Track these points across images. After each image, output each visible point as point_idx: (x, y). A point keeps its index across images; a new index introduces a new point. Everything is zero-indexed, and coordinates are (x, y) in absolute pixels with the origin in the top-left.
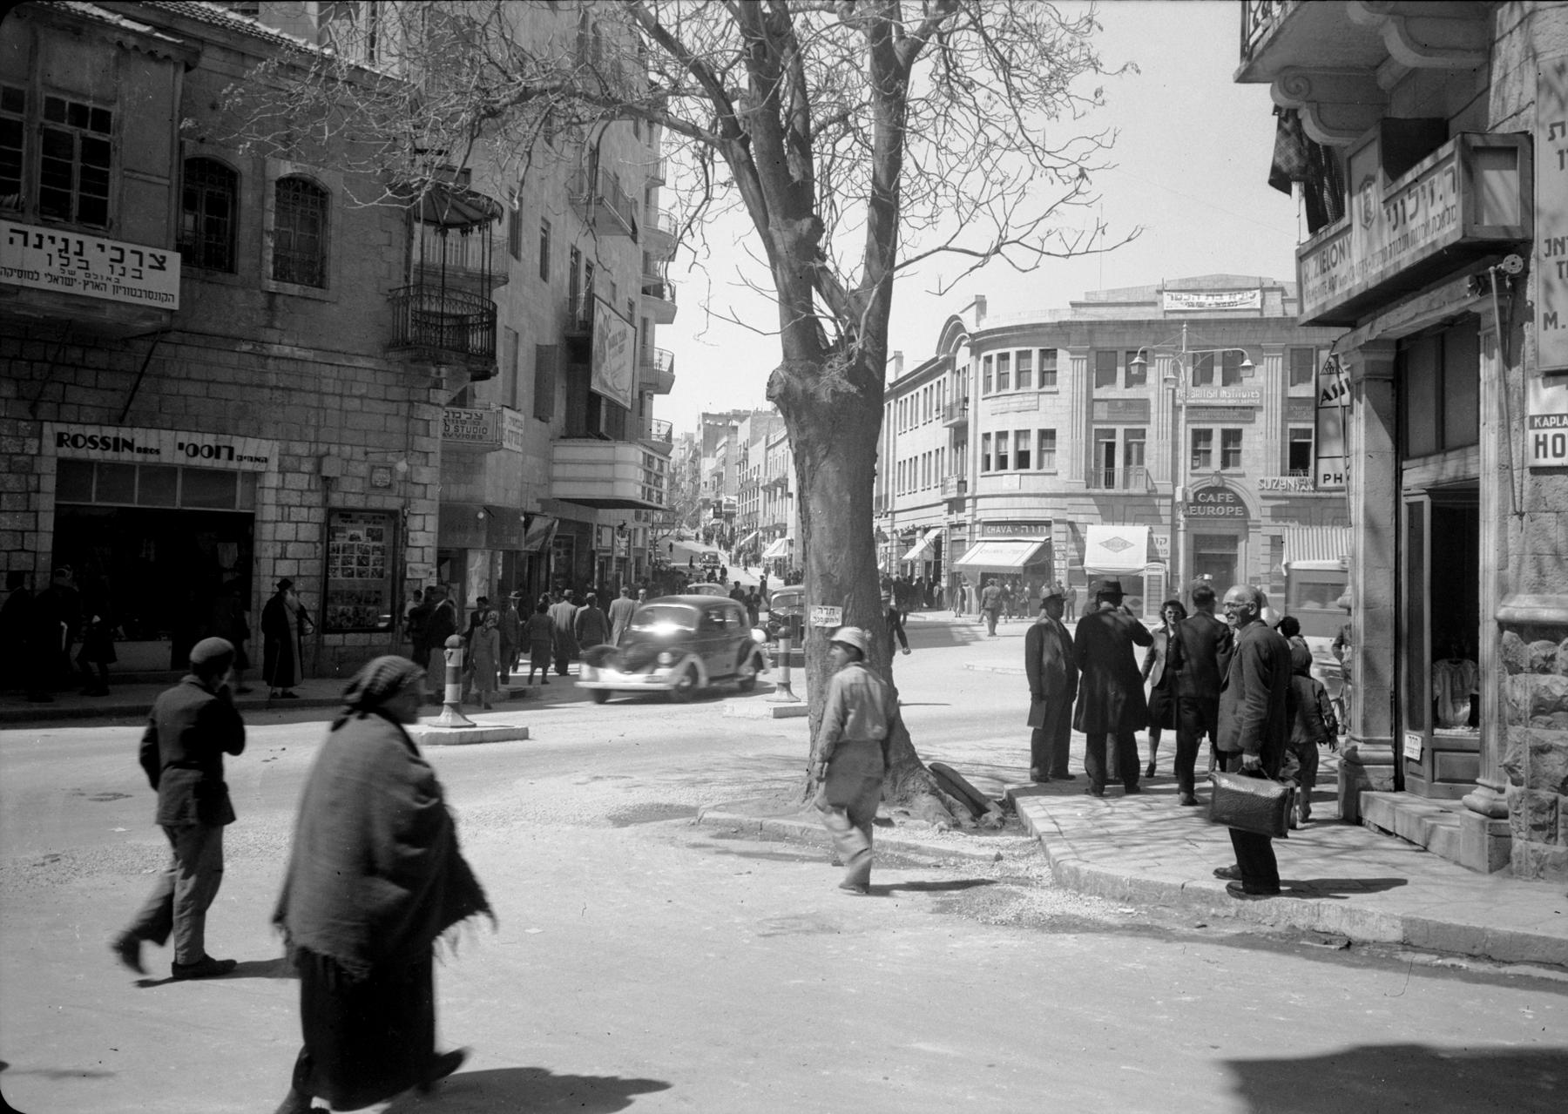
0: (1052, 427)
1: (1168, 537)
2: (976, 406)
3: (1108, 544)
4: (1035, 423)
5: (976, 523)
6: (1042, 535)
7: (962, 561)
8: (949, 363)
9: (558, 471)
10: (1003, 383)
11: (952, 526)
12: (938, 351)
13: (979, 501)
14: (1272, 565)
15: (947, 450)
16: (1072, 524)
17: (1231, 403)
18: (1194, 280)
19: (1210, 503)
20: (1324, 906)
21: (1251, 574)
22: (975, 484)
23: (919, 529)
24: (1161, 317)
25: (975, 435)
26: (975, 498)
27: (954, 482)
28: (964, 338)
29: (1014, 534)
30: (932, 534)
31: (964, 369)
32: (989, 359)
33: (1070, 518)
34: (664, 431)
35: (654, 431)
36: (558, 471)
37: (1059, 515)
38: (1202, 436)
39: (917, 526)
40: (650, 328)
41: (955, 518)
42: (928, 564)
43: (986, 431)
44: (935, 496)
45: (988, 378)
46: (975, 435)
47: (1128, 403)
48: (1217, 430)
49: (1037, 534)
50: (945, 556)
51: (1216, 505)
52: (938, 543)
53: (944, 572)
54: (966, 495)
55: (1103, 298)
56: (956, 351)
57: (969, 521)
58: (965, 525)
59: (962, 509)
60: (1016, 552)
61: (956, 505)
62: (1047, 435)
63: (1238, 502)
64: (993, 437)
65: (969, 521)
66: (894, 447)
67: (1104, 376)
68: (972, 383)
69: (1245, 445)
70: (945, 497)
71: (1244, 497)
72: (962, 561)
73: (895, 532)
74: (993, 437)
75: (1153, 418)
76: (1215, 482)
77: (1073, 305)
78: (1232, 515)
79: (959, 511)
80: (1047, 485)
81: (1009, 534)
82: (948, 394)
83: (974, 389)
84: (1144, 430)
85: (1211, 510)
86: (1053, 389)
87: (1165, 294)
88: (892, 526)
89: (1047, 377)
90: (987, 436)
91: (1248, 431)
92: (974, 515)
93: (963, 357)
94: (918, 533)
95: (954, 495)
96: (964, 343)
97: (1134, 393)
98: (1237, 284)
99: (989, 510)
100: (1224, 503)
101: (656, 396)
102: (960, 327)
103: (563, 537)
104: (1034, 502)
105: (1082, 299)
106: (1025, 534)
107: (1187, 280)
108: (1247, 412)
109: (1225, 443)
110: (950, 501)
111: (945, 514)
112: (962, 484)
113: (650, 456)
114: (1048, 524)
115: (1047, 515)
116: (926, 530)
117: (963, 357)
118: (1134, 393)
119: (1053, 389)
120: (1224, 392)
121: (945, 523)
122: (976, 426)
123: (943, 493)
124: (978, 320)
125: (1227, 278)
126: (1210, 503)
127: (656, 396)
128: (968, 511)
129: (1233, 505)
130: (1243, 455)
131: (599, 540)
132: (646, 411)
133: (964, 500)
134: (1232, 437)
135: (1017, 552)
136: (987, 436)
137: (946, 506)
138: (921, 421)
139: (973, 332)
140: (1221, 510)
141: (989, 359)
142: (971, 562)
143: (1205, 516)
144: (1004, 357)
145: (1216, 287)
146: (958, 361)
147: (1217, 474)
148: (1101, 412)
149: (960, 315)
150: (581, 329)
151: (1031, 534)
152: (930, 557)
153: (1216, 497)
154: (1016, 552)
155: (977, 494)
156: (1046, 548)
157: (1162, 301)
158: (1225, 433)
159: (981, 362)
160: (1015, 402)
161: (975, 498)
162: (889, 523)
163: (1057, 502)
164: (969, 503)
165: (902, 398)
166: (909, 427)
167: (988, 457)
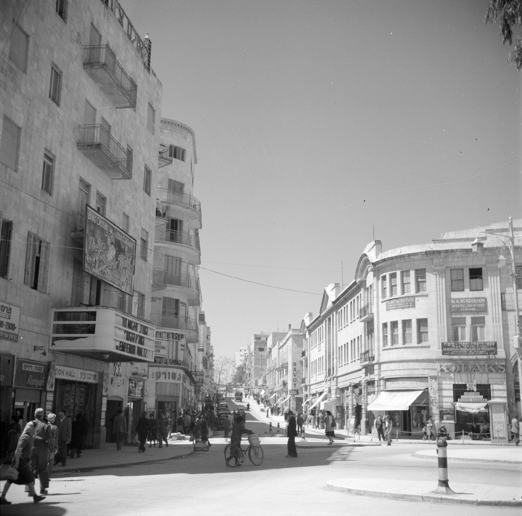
0: (426, 317)
2: (378, 307)
5: (380, 379)
8: (363, 283)
12: (356, 278)
13: (382, 366)
22: (379, 355)
25: (378, 325)
26: (380, 364)
32: (384, 278)
41: (370, 377)
43: (385, 322)
44: (358, 365)
45: (384, 289)
46: (378, 325)
53: (363, 412)
54: (374, 362)
56: (366, 277)
57: (376, 378)
59: (372, 372)
61: (369, 369)
62: (422, 322)
64: (389, 325)
65: (376, 378)
68: (375, 293)
75: (490, 309)
79: (371, 374)
82: (362, 302)
84: (484, 318)
88: (337, 385)
90: (385, 325)
92: (379, 375)
93: (370, 279)
99: (387, 371)
102: (367, 261)
115: (426, 373)
117: (370, 279)
119: (424, 293)
122: (378, 319)
124: (377, 255)
128: (376, 372)
133: (373, 365)
136: (385, 325)
137: (364, 370)
155: (380, 361)
156: (426, 393)
161: (380, 364)
163: (431, 365)
164: (376, 367)
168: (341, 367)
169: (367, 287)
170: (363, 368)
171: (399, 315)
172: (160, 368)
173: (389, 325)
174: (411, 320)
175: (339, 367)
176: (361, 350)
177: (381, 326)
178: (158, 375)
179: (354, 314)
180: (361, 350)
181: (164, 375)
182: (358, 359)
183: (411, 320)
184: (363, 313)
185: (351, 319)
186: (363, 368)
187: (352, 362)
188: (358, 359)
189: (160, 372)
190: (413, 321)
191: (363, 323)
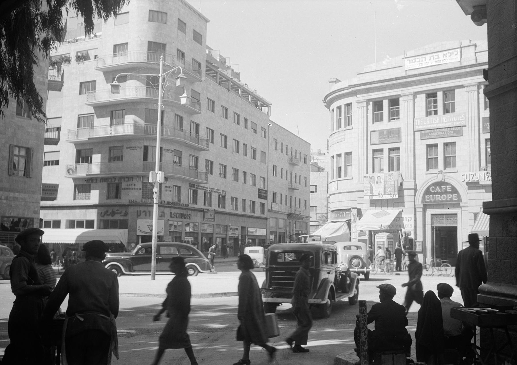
17: (448, 125)
19: (437, 193)
47: (390, 132)
48: (440, 142)
51: (441, 193)
63: (454, 191)
74: (343, 155)
85: (438, 197)
89: (349, 122)
97: (394, 125)
100: (446, 192)
108: (458, 130)
118: (394, 125)
126: (437, 193)
129: (451, 193)
130: (457, 159)
148: (375, 138)
153: (441, 188)
167: (340, 168)
172: (141, 207)
178: (139, 214)
181: (144, 213)
189: (140, 211)
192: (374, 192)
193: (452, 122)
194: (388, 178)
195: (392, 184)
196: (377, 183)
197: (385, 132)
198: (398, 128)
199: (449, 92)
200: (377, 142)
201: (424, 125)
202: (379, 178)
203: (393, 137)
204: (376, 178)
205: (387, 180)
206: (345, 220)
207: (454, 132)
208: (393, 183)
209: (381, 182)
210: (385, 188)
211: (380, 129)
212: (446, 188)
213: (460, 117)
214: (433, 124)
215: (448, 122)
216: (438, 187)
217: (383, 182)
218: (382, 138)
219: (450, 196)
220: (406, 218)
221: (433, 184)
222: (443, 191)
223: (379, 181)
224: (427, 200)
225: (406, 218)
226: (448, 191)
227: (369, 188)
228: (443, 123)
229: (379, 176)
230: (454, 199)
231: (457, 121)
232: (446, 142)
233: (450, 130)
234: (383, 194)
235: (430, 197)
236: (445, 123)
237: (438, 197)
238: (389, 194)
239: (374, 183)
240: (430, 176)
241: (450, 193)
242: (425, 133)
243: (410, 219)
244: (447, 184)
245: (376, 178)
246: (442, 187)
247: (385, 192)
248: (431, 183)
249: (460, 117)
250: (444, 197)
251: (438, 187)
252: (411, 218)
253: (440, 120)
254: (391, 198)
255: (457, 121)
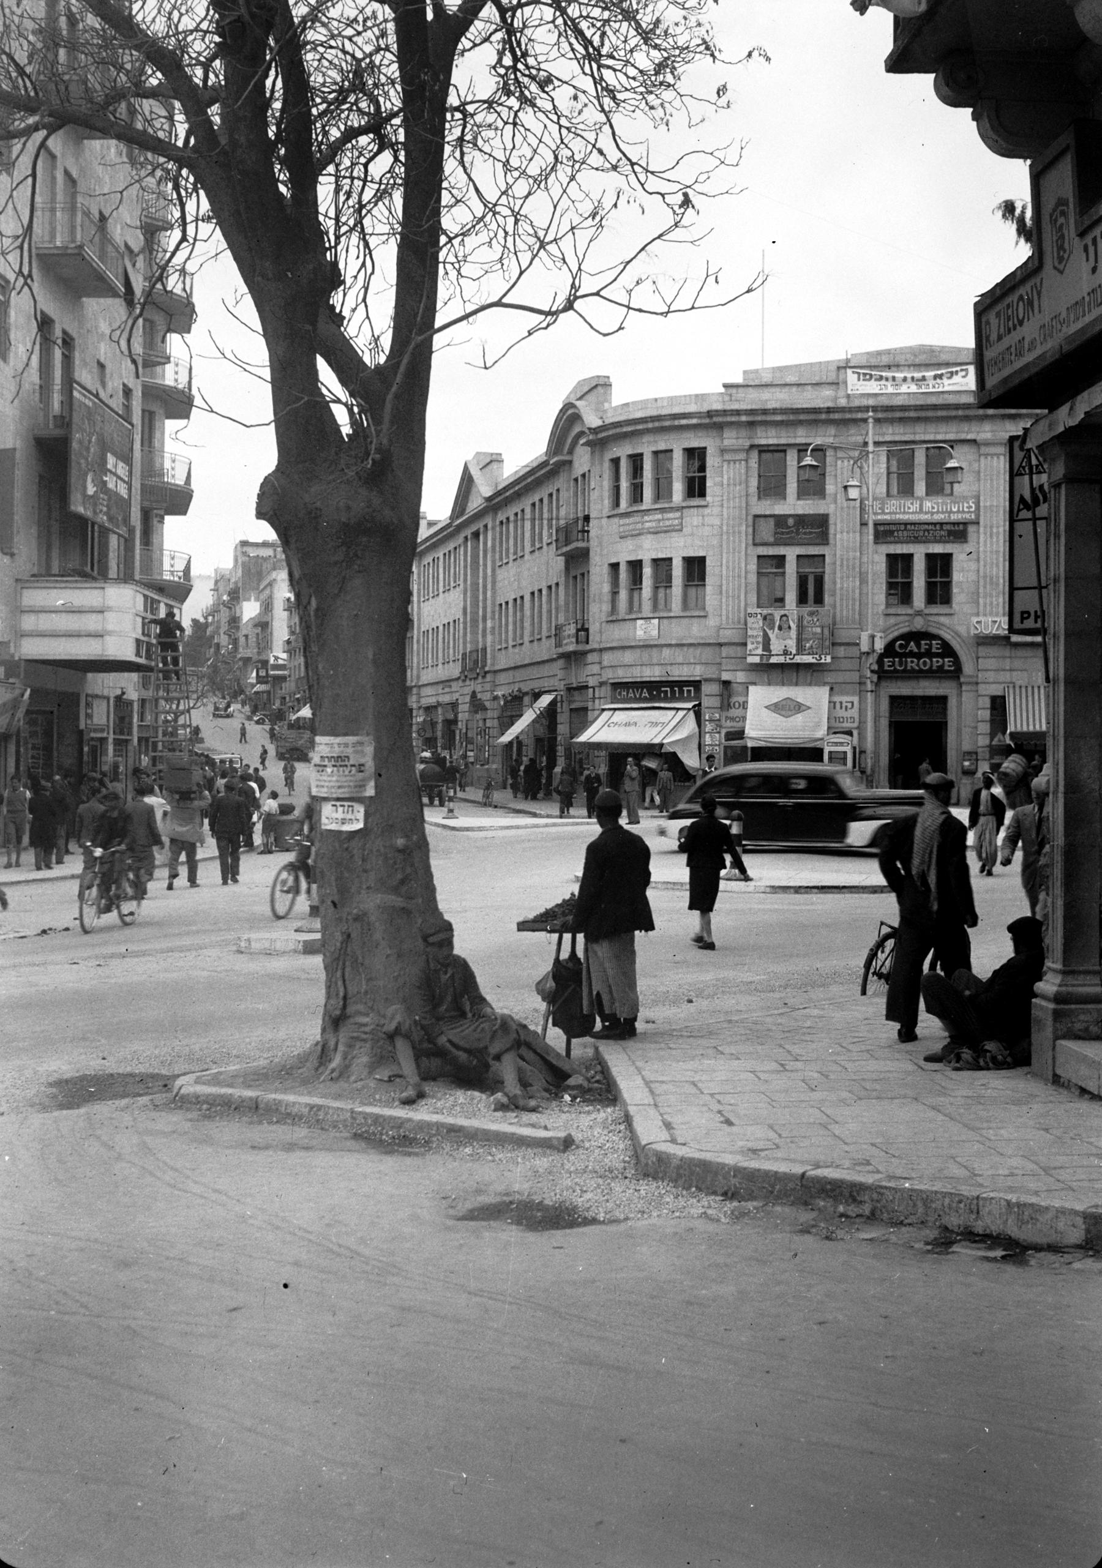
0: (701, 554)
1: (856, 699)
3: (777, 708)
4: (678, 549)
5: (602, 684)
6: (688, 700)
7: (583, 738)
9: (28, 622)
10: (637, 494)
11: (570, 689)
14: (992, 735)
15: (562, 588)
16: (727, 684)
18: (888, 352)
19: (912, 654)
20: (985, 1199)
21: (967, 747)
23: (527, 693)
24: (843, 402)
27: (571, 630)
28: (581, 434)
29: (652, 699)
30: (545, 700)
31: (584, 475)
33: (725, 676)
34: (180, 566)
35: (166, 566)
36: (28, 622)
37: (711, 673)
38: (899, 565)
39: (525, 689)
40: (157, 424)
42: (538, 740)
44: (546, 649)
47: (802, 520)
48: (919, 552)
49: (682, 699)
50: (562, 729)
51: (919, 656)
52: (551, 712)
53: (561, 751)
55: (767, 378)
56: (571, 452)
58: (587, 687)
60: (655, 724)
61: (574, 659)
62: (696, 567)
63: (948, 650)
64: (623, 568)
65: (592, 682)
66: (494, 583)
67: (772, 487)
69: (957, 576)
70: (560, 650)
71: (955, 644)
72: (583, 738)
73: (496, 698)
76: (918, 624)
77: (725, 386)
78: (941, 669)
80: (696, 631)
81: (645, 700)
82: (563, 512)
83: (599, 502)
85: (912, 663)
86: (703, 503)
87: (849, 371)
89: (696, 488)
91: (960, 554)
94: (527, 700)
95: (571, 648)
96: (582, 441)
98: (944, 358)
100: (929, 654)
101: (167, 518)
102: (576, 418)
103: (38, 712)
104: (679, 656)
105: (739, 379)
106: (666, 699)
107: (879, 353)
109: (931, 571)
110: (567, 657)
111: (560, 674)
112: (583, 630)
113: (153, 601)
114: (697, 685)
115: (696, 672)
116: (537, 696)
117: (582, 460)
119: (703, 503)
120: (928, 505)
121: (561, 686)
123: (558, 645)
125: (931, 350)
126: (912, 654)
127: (167, 518)
131: (89, 716)
132: (155, 540)
134: (940, 566)
135: (656, 724)
136: (615, 566)
138: (528, 548)
139: (594, 426)
140: (925, 663)
141: (616, 462)
142: (595, 739)
143: (904, 671)
144: (636, 461)
145: (917, 361)
146: (576, 464)
147: (919, 613)
148: (767, 531)
149: (578, 403)
150: (56, 426)
151: (673, 699)
152: (542, 731)
153: (918, 646)
154: (655, 724)
157: (845, 383)
158: (930, 557)
159: (607, 465)
160: (650, 522)
162: (488, 687)
165: (501, 516)
166: (512, 557)
168: (503, 652)
169: (574, 477)
170: (559, 658)
171: (648, 550)
173: (623, 568)
174: (670, 559)
175: (500, 650)
176: (557, 617)
177: (606, 570)
179: (541, 534)
180: (557, 617)
182: (549, 637)
183: (670, 559)
184: (562, 538)
185: (533, 545)
186: (559, 658)
187: (532, 642)
188: (549, 637)
190: (675, 562)
191: (563, 558)
192: (772, 647)
193: (947, 512)
194: (807, 618)
195: (816, 634)
196: (780, 628)
197: (791, 522)
198: (823, 515)
199: (938, 452)
200: (772, 540)
201: (883, 513)
202: (784, 618)
203: (811, 533)
204: (777, 618)
205: (805, 623)
206: (690, 705)
207: (950, 533)
208: (819, 630)
209: (790, 627)
210: (800, 641)
211: (776, 513)
212: (931, 645)
213: (966, 505)
214: (904, 513)
215: (938, 512)
216: (912, 643)
217: (793, 626)
218: (783, 533)
219: (936, 662)
220: (841, 703)
221: (901, 637)
222: (923, 650)
223: (786, 626)
224: (886, 668)
225: (841, 703)
226: (934, 650)
227: (760, 639)
228: (926, 513)
229: (785, 615)
230: (946, 668)
231: (958, 512)
232: (930, 551)
233: (942, 529)
234: (794, 652)
235: (894, 663)
236: (932, 514)
237: (912, 662)
238: (809, 654)
239: (772, 628)
240: (892, 620)
241: (937, 655)
242: (884, 532)
243: (849, 705)
244: (931, 636)
245: (777, 618)
246: (923, 642)
247: (800, 650)
248: (896, 634)
249: (966, 505)
250: (925, 663)
251: (912, 643)
252: (852, 703)
253: (921, 506)
254: (814, 661)
255: (958, 512)
